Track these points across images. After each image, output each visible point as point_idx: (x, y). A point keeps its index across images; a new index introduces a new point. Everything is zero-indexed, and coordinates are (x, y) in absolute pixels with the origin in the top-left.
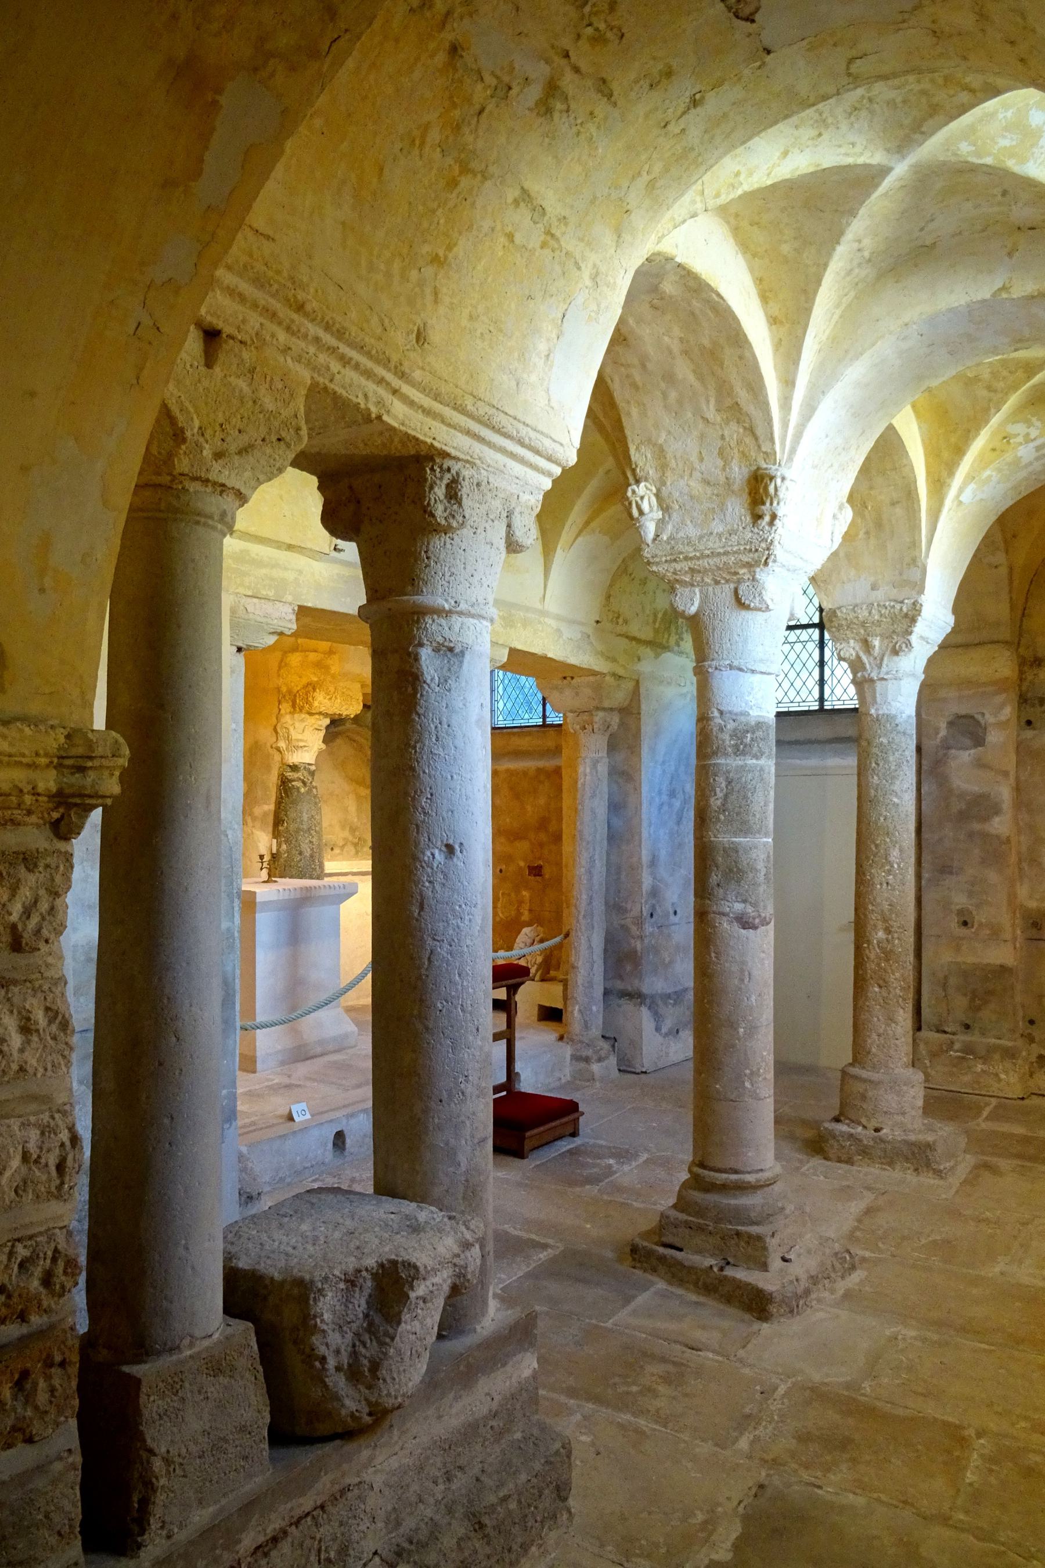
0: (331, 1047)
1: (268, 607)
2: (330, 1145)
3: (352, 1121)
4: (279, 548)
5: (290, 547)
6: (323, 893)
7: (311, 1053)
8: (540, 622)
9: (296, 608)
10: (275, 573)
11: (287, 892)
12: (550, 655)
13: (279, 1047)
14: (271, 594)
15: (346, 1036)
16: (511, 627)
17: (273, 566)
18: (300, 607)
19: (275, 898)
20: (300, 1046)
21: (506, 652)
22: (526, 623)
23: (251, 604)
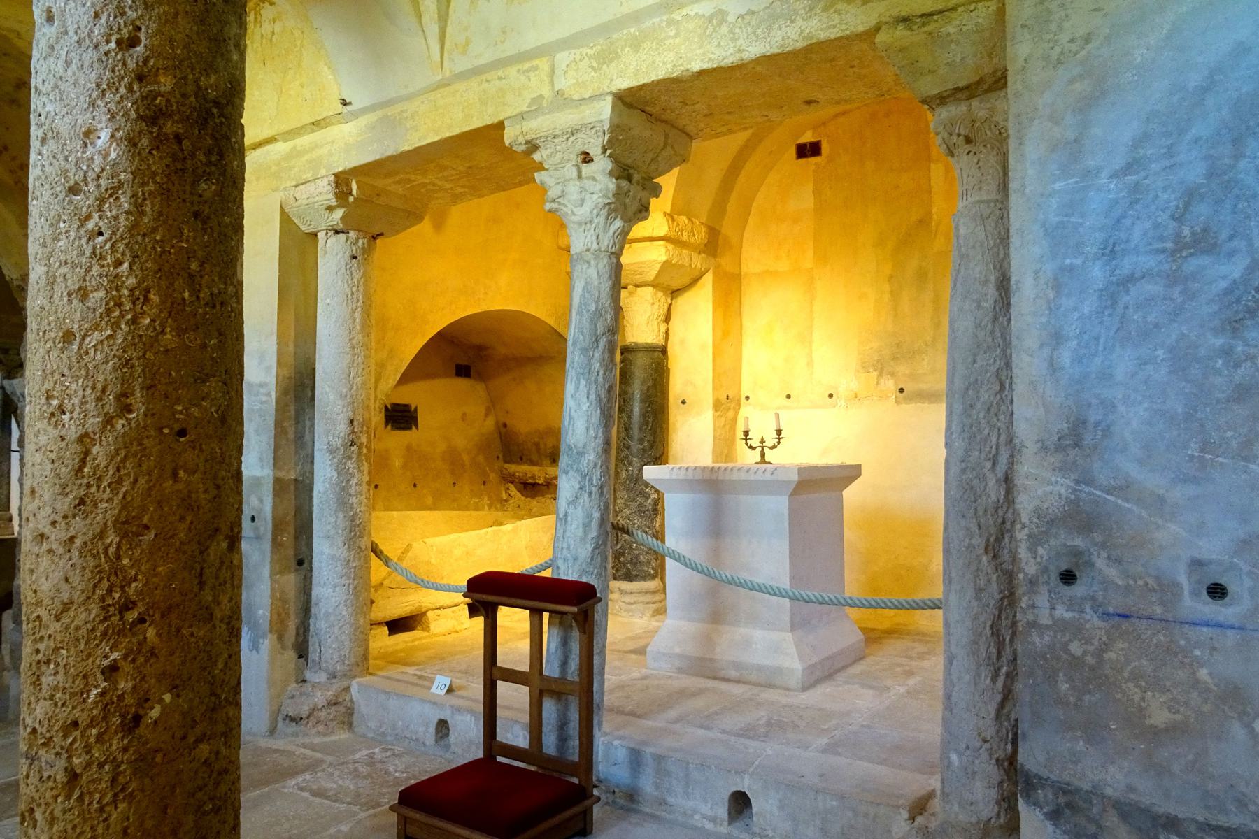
0: (753, 678)
1: (310, 188)
2: (432, 729)
3: (458, 717)
4: (313, 131)
5: (317, 125)
6: (735, 476)
7: (722, 674)
8: (670, 23)
9: (332, 178)
10: (314, 155)
11: (683, 472)
12: (696, 66)
13: (677, 650)
14: (309, 176)
15: (779, 671)
16: (611, 61)
17: (313, 149)
18: (336, 175)
19: (667, 477)
20: (702, 659)
21: (609, 99)
22: (636, 44)
23: (302, 193)
